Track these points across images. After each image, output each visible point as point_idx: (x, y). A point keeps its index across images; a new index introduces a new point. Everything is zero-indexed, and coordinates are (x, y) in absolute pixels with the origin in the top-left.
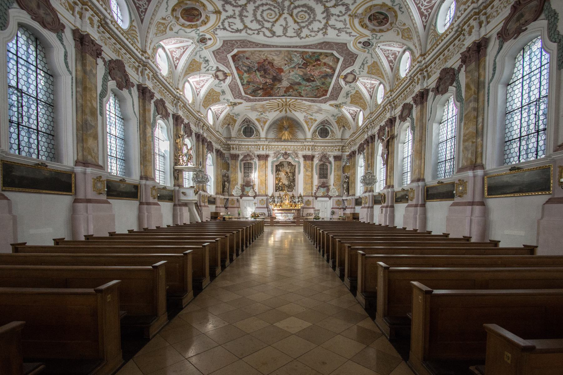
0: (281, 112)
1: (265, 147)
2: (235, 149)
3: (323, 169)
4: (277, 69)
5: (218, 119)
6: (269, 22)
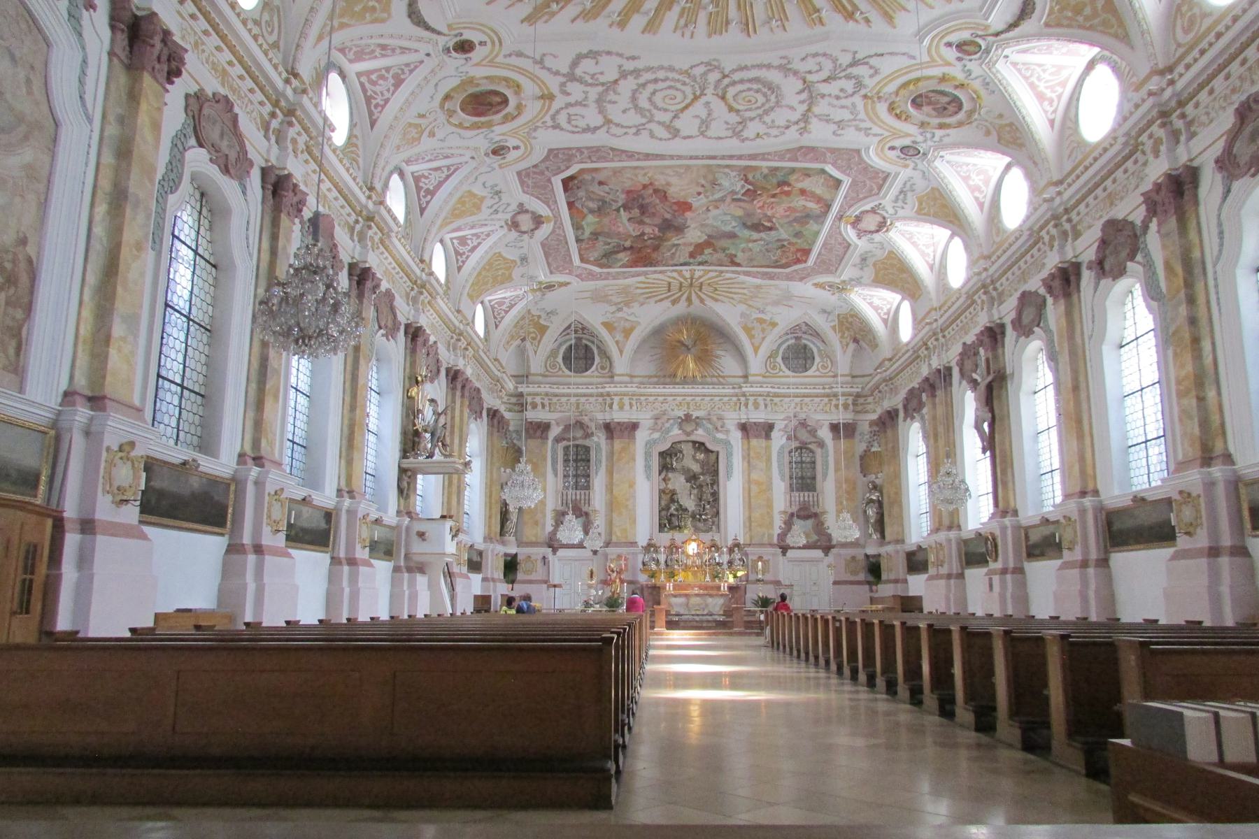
0: (674, 302)
1: (626, 400)
2: (540, 407)
3: (802, 462)
4: (675, 203)
5: (497, 326)
6: (666, 110)
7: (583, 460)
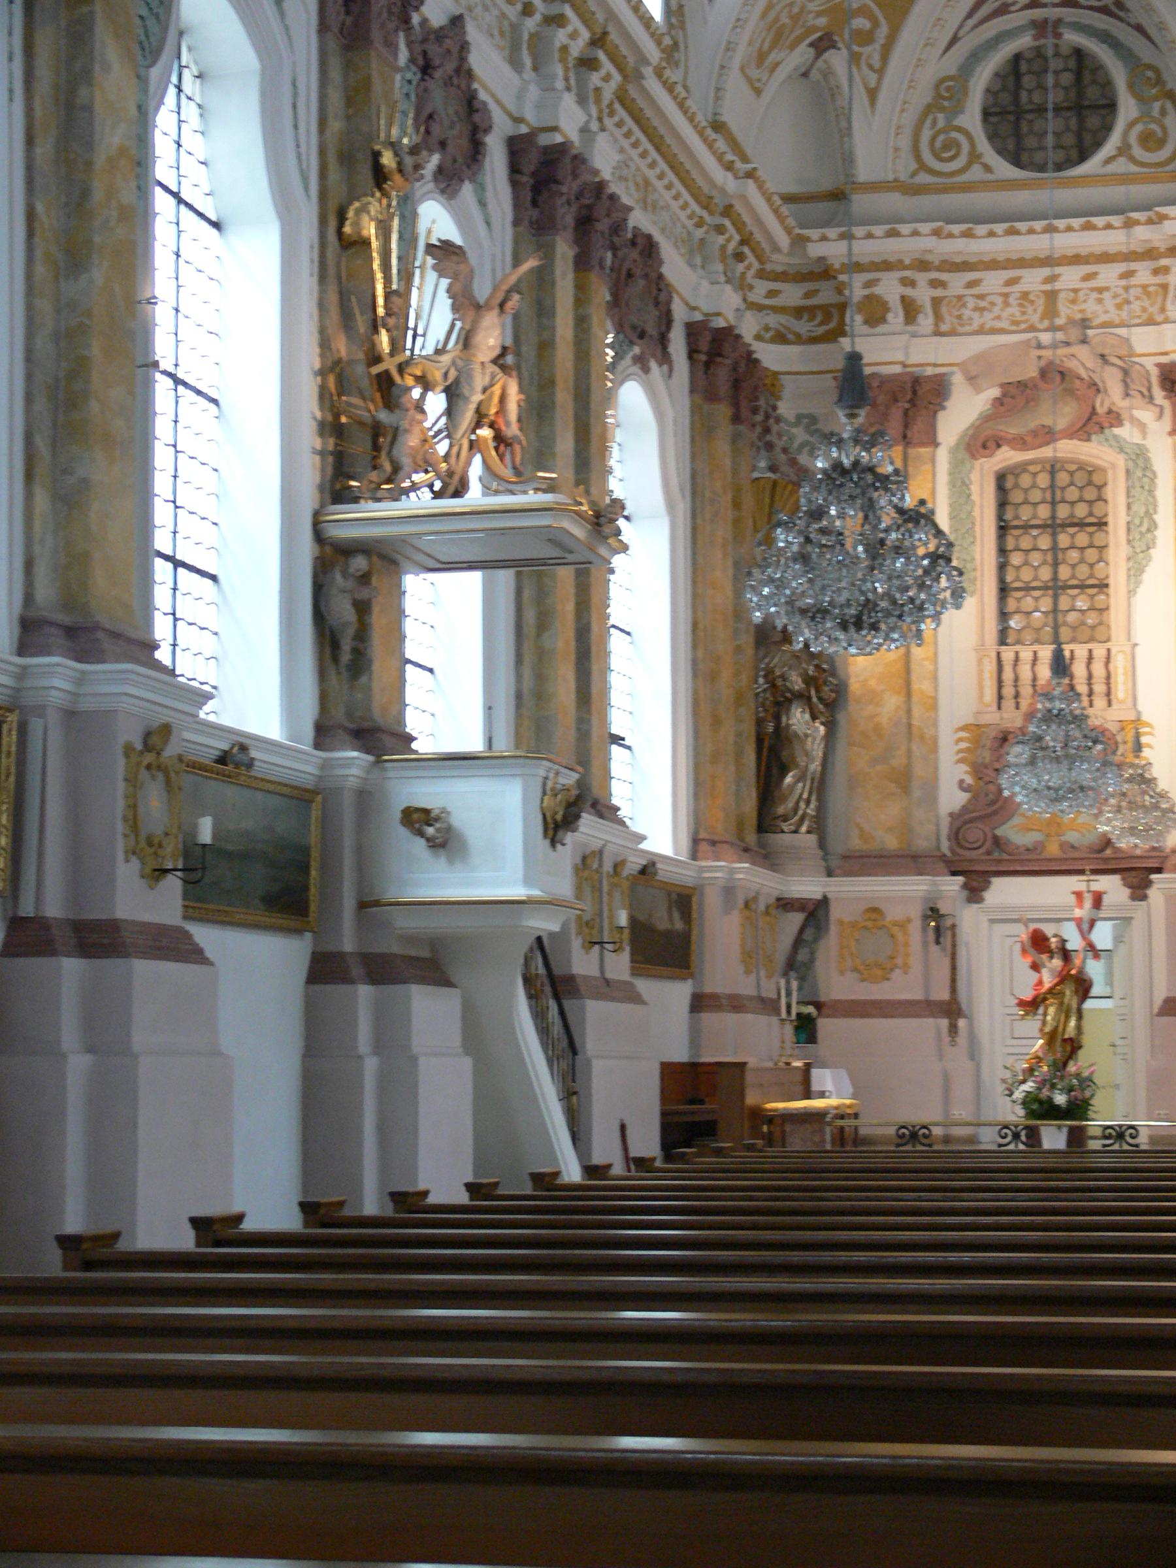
2: (896, 318)
7: (1081, 525)
